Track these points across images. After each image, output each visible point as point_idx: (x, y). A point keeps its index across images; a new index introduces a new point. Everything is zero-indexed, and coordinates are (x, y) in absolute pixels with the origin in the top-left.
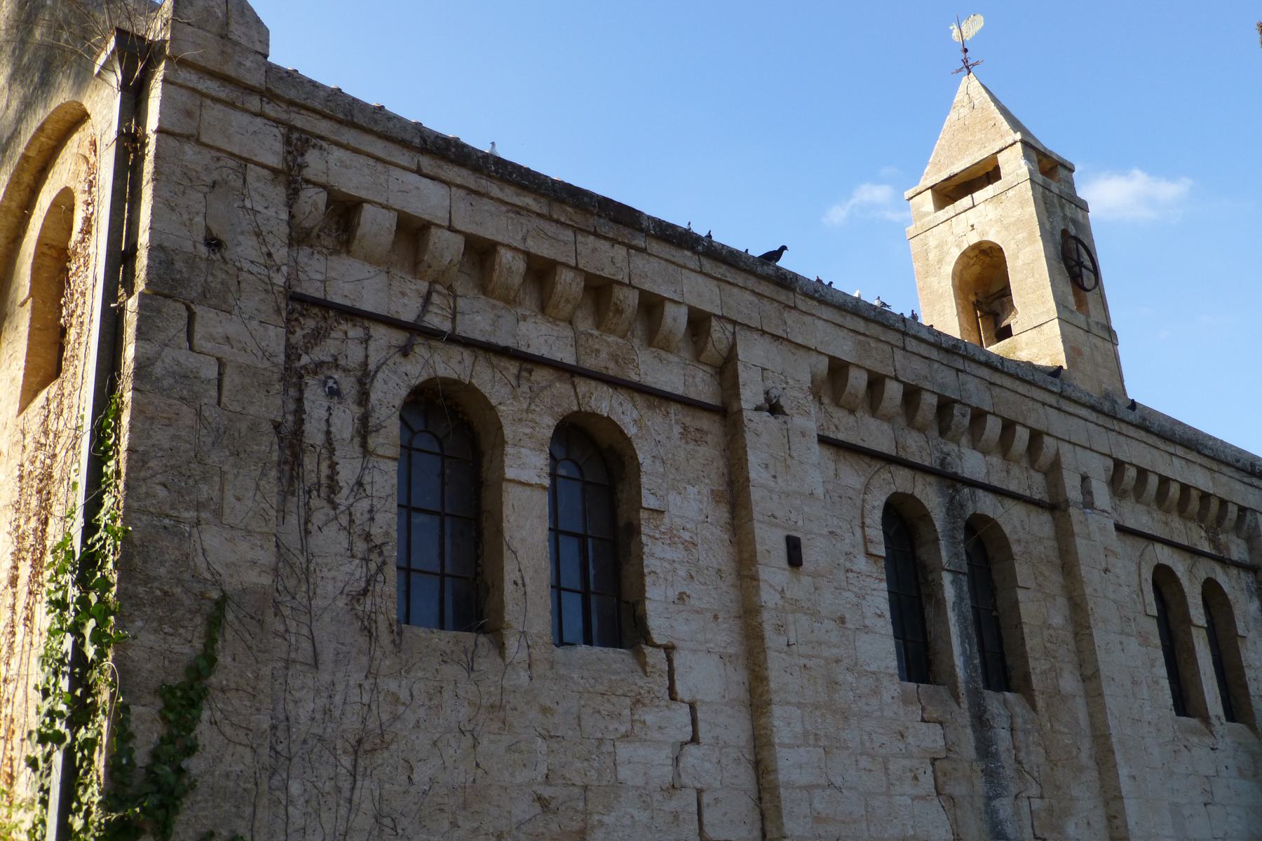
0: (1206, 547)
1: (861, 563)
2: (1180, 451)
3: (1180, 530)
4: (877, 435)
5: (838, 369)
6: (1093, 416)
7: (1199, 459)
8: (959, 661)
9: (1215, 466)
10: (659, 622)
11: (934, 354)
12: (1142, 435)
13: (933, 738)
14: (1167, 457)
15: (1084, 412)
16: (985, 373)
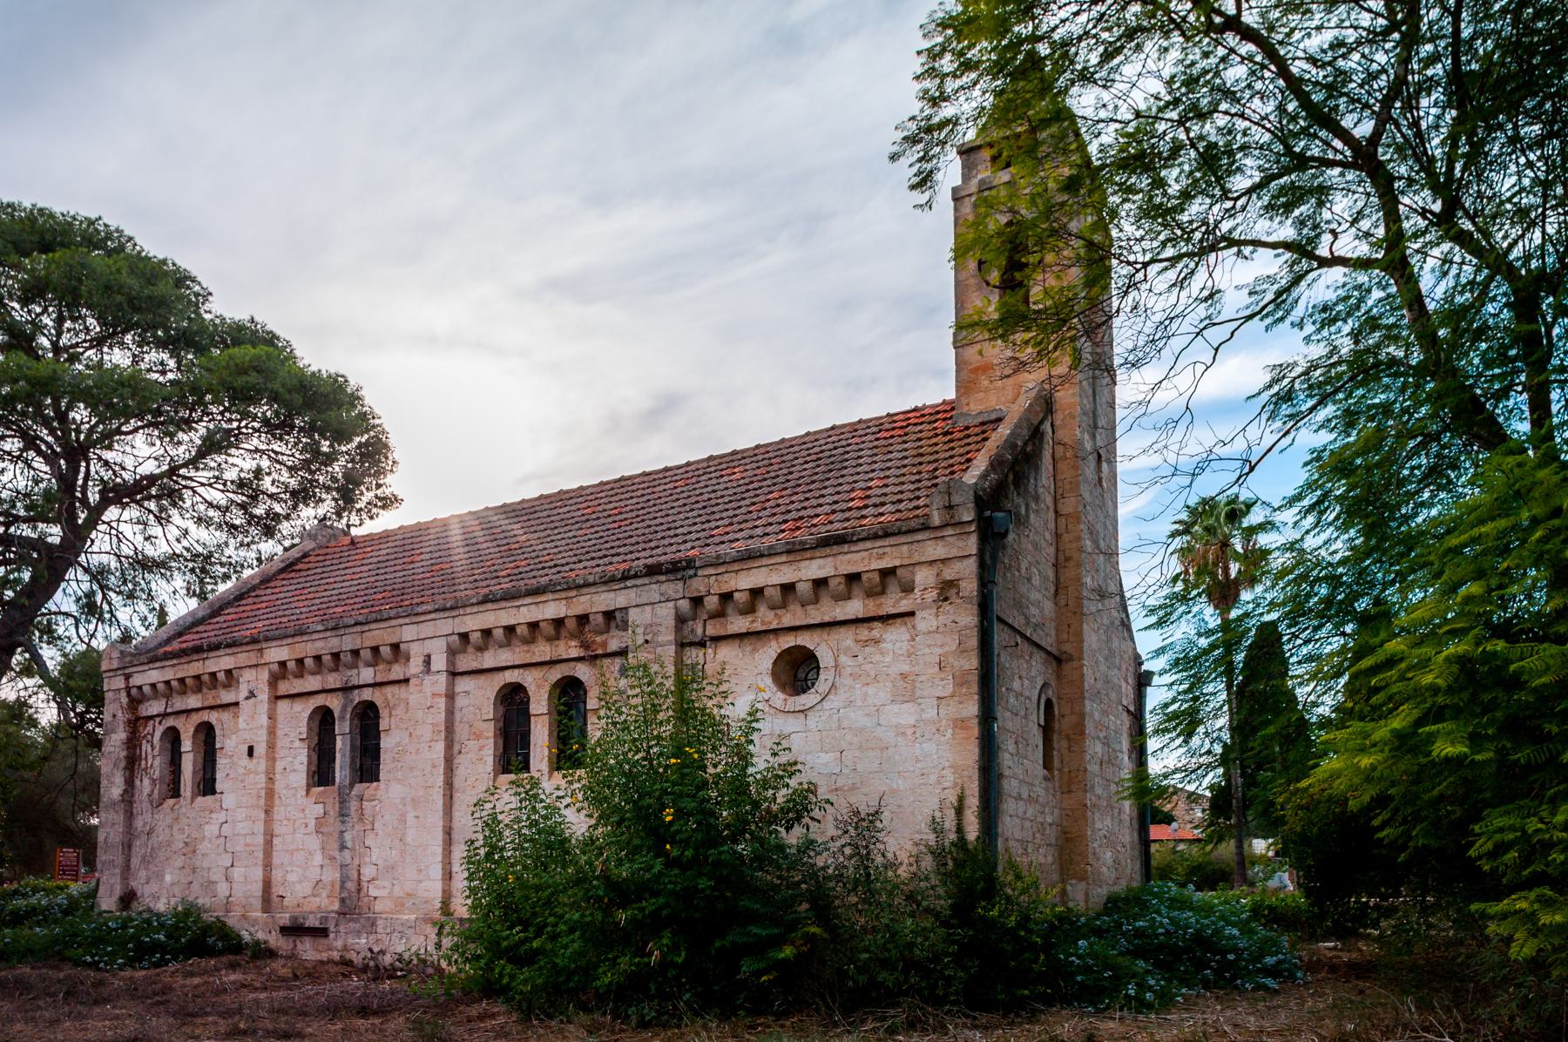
0: (574, 653)
1: (297, 744)
2: (528, 600)
3: (543, 651)
4: (312, 683)
5: (283, 664)
6: (441, 615)
7: (551, 596)
8: (337, 775)
9: (573, 593)
10: (218, 787)
11: (329, 634)
12: (490, 606)
13: (319, 809)
14: (514, 611)
15: (433, 616)
16: (358, 628)
